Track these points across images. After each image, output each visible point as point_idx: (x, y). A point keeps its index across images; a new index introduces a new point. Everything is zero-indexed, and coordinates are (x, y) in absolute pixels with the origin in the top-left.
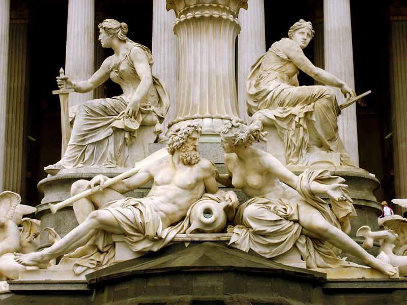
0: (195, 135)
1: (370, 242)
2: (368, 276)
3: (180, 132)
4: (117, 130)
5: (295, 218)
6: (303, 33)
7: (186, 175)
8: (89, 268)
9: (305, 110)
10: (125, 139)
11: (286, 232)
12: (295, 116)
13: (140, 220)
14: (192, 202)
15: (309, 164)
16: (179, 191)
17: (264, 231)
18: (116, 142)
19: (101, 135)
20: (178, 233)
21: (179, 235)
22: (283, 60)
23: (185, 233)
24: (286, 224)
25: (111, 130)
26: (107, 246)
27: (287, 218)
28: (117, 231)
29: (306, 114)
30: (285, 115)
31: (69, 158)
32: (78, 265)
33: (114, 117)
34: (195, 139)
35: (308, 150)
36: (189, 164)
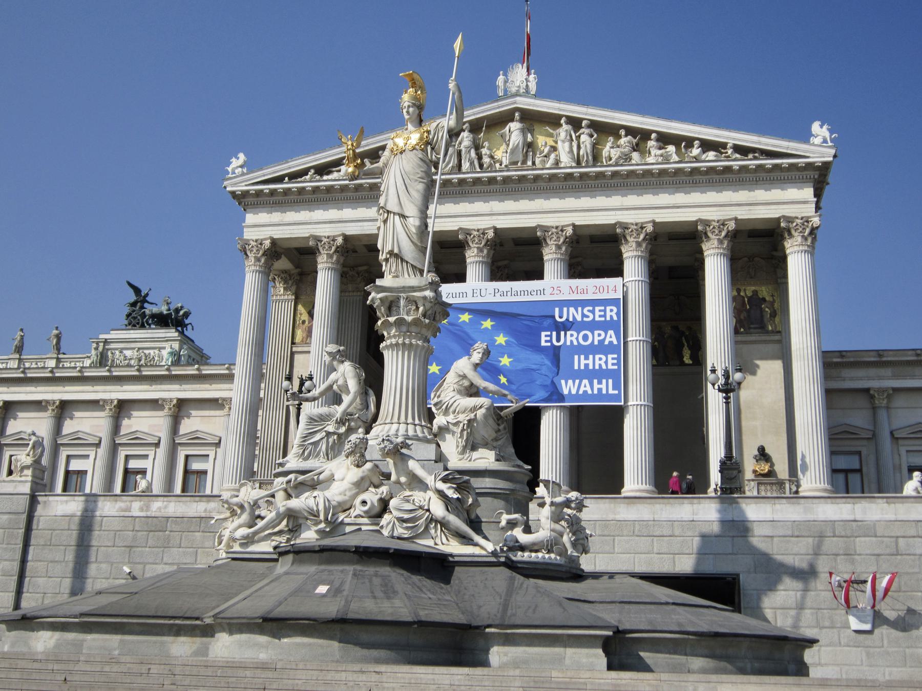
0: (361, 446)
1: (503, 523)
2: (476, 551)
3: (350, 443)
4: (328, 434)
5: (426, 507)
6: (479, 353)
7: (355, 474)
8: (281, 543)
9: (468, 418)
10: (334, 440)
11: (420, 518)
12: (461, 422)
13: (315, 509)
14: (357, 494)
15: (473, 459)
16: (352, 486)
17: (403, 517)
18: (328, 442)
19: (317, 437)
20: (346, 517)
21: (345, 519)
22: (460, 376)
23: (351, 517)
24: (420, 512)
25: (324, 434)
26: (297, 526)
27: (421, 507)
28: (301, 516)
29: (469, 421)
30: (455, 421)
31: (295, 454)
32: (273, 540)
33: (327, 423)
34: (361, 448)
35: (474, 448)
36: (358, 466)
